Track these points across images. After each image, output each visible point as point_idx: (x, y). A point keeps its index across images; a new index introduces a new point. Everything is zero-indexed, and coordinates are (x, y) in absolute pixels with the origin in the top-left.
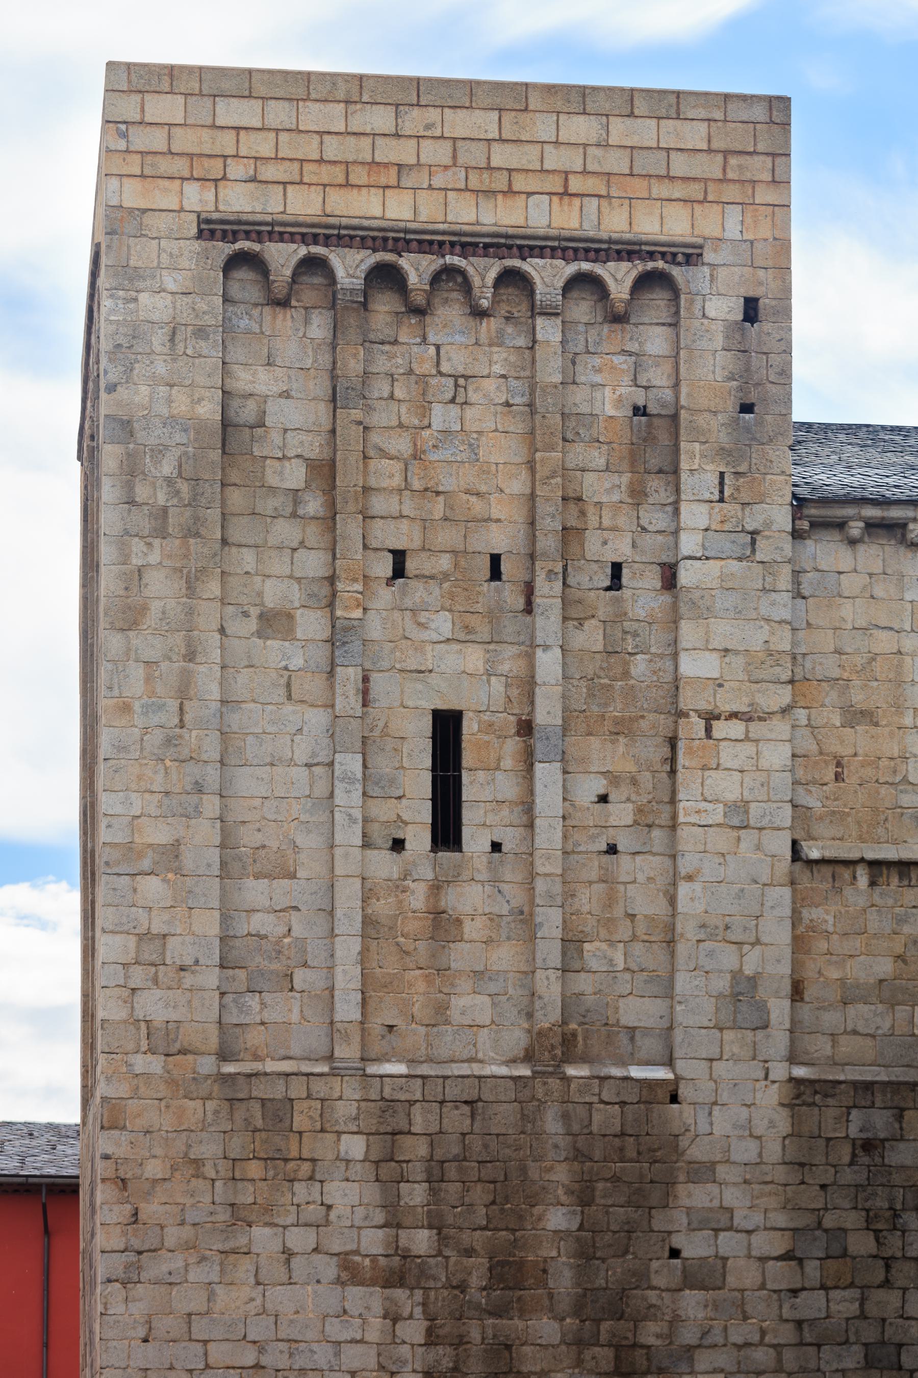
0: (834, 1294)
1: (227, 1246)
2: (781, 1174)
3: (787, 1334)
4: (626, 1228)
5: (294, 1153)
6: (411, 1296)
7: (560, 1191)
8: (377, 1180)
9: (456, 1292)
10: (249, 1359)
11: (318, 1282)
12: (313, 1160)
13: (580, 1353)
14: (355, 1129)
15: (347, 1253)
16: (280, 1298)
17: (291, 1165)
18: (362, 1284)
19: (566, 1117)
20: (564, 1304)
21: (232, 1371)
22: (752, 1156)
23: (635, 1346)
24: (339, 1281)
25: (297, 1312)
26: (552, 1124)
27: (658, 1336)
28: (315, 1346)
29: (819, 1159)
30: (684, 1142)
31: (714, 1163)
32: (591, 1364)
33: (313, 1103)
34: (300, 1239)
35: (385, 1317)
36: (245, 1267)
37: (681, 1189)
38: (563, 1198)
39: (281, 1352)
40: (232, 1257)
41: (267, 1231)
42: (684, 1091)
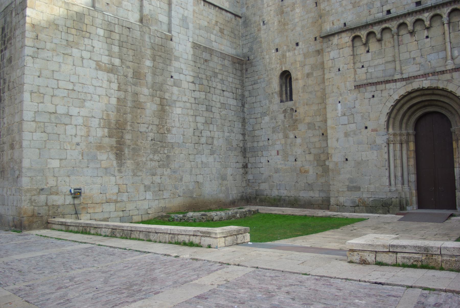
0: (201, 93)
1: (65, 52)
2: (192, 63)
3: (192, 100)
4: (162, 69)
5: (85, 30)
6: (114, 76)
7: (149, 56)
8: (106, 43)
9: (125, 77)
10: (71, 87)
11: (90, 68)
12: (90, 33)
13: (153, 98)
14: (101, 27)
15: (98, 61)
16: (79, 70)
17: (84, 33)
18: (102, 70)
19: (150, 38)
20: (149, 86)
21: (65, 90)
22: (186, 57)
23: (164, 98)
24: (96, 69)
25: (85, 76)
26: (147, 39)
27: (169, 97)
28: (89, 86)
29: (198, 61)
30: (174, 50)
31: (179, 57)
32: (155, 102)
33: (90, 17)
34: (86, 55)
35: (108, 81)
36: (70, 59)
37: (173, 62)
38: (149, 58)
39: (80, 87)
40: (66, 56)
41: (77, 50)
42: (173, 39)
